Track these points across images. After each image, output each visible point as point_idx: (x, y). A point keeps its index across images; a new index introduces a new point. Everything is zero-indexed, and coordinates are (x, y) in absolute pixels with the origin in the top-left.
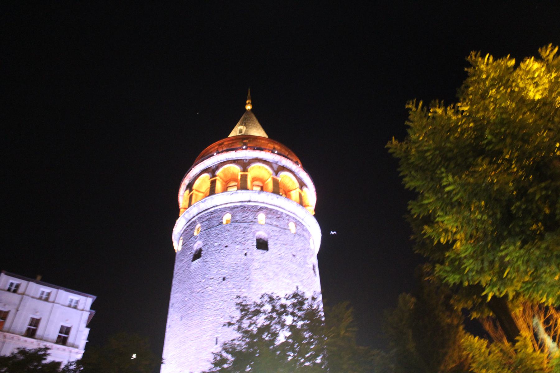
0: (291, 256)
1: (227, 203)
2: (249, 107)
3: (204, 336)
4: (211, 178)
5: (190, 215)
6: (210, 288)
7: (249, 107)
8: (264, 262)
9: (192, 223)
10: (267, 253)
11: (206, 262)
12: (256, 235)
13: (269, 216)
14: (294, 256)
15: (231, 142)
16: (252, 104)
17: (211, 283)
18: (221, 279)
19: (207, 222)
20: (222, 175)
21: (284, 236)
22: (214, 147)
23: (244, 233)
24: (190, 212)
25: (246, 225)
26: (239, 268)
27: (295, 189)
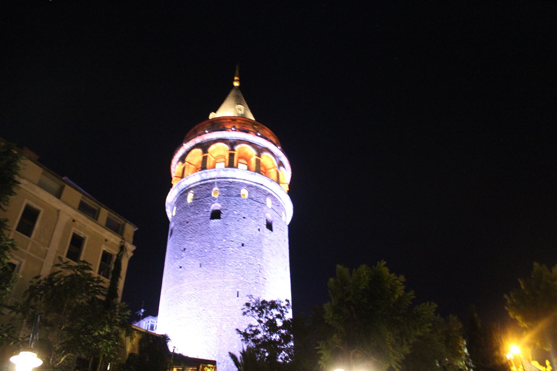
1: (245, 180)
3: (227, 287)
4: (230, 150)
6: (231, 248)
7: (236, 84)
9: (207, 183)
11: (226, 225)
16: (240, 81)
17: (232, 245)
18: (240, 245)
19: (225, 189)
23: (258, 211)
24: (209, 174)
25: (258, 204)
26: (254, 240)
27: (284, 183)
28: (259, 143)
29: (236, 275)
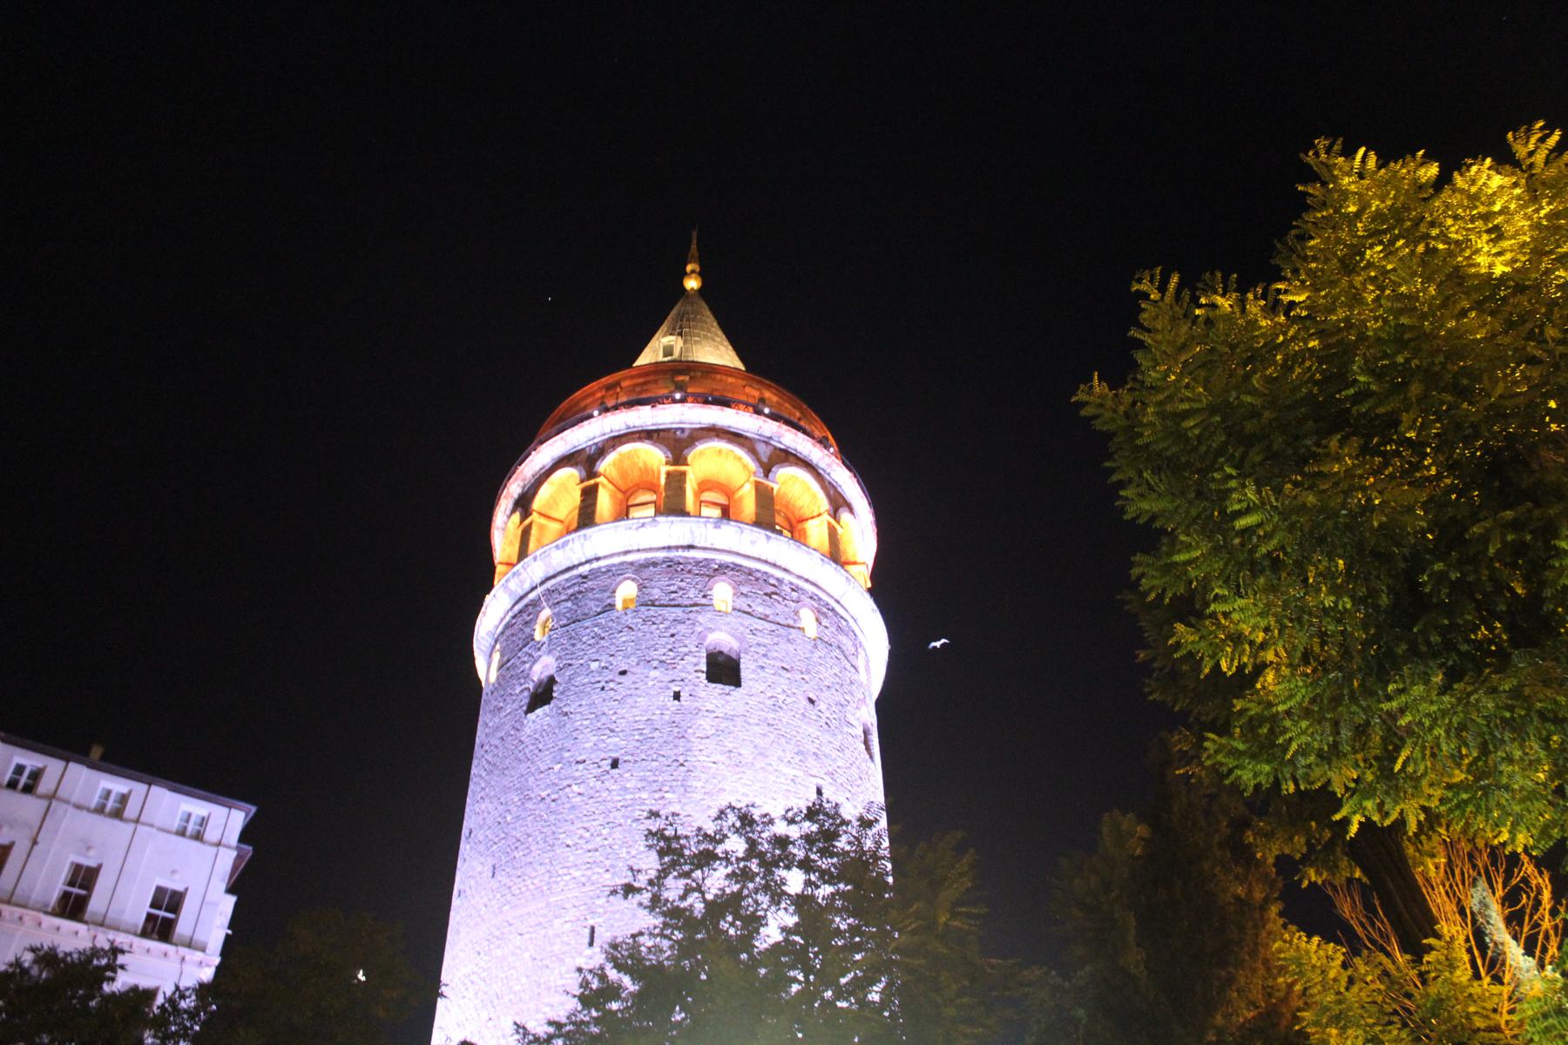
0: (806, 703)
1: (626, 553)
2: (692, 284)
3: (557, 922)
4: (582, 481)
5: (522, 582)
6: (575, 788)
7: (692, 284)
8: (726, 718)
9: (527, 606)
10: (737, 693)
11: (566, 714)
12: (706, 643)
13: (745, 589)
14: (811, 701)
15: (641, 380)
16: (702, 274)
17: (577, 774)
18: (606, 765)
19: (569, 604)
20: (614, 473)
21: (784, 645)
22: (593, 394)
23: (673, 636)
24: (524, 575)
26: (657, 734)
27: (819, 515)
28: (680, 423)
29: (589, 873)
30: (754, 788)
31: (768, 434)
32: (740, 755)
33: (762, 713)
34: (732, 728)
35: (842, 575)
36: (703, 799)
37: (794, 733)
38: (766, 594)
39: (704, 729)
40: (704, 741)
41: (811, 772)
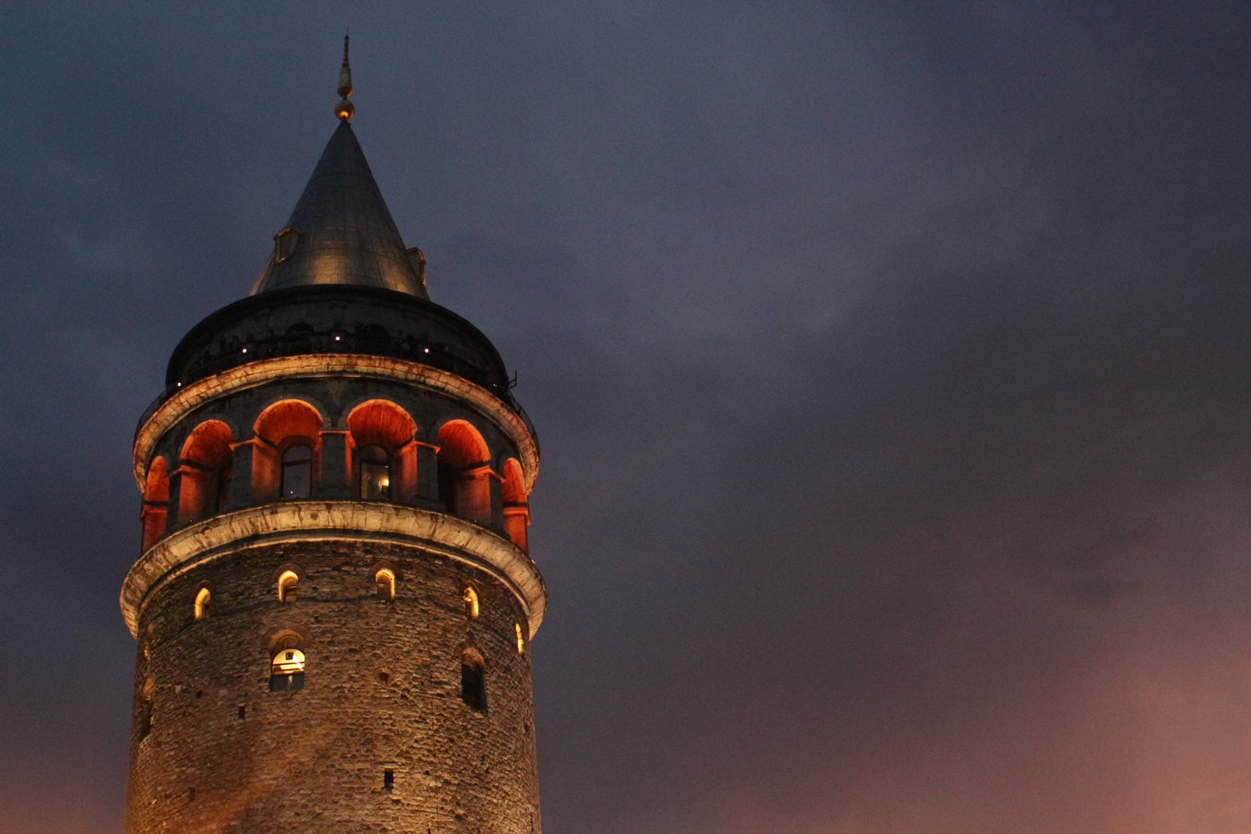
8: (290, 726)
13: (310, 572)
14: (384, 677)
25: (244, 617)
26: (225, 758)
30: (313, 796)
31: (338, 368)
32: (300, 763)
33: (324, 711)
34: (293, 736)
35: (424, 515)
36: (265, 821)
37: (361, 722)
38: (334, 569)
39: (266, 745)
40: (265, 758)
41: (381, 760)
